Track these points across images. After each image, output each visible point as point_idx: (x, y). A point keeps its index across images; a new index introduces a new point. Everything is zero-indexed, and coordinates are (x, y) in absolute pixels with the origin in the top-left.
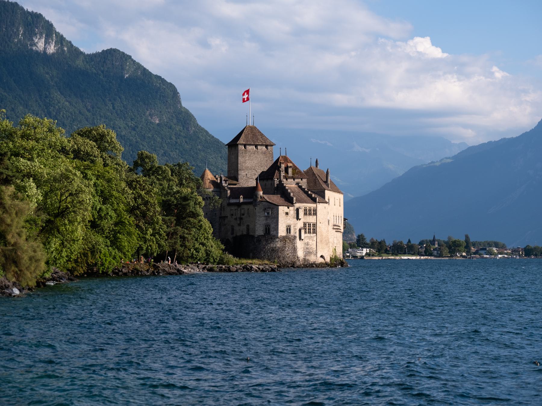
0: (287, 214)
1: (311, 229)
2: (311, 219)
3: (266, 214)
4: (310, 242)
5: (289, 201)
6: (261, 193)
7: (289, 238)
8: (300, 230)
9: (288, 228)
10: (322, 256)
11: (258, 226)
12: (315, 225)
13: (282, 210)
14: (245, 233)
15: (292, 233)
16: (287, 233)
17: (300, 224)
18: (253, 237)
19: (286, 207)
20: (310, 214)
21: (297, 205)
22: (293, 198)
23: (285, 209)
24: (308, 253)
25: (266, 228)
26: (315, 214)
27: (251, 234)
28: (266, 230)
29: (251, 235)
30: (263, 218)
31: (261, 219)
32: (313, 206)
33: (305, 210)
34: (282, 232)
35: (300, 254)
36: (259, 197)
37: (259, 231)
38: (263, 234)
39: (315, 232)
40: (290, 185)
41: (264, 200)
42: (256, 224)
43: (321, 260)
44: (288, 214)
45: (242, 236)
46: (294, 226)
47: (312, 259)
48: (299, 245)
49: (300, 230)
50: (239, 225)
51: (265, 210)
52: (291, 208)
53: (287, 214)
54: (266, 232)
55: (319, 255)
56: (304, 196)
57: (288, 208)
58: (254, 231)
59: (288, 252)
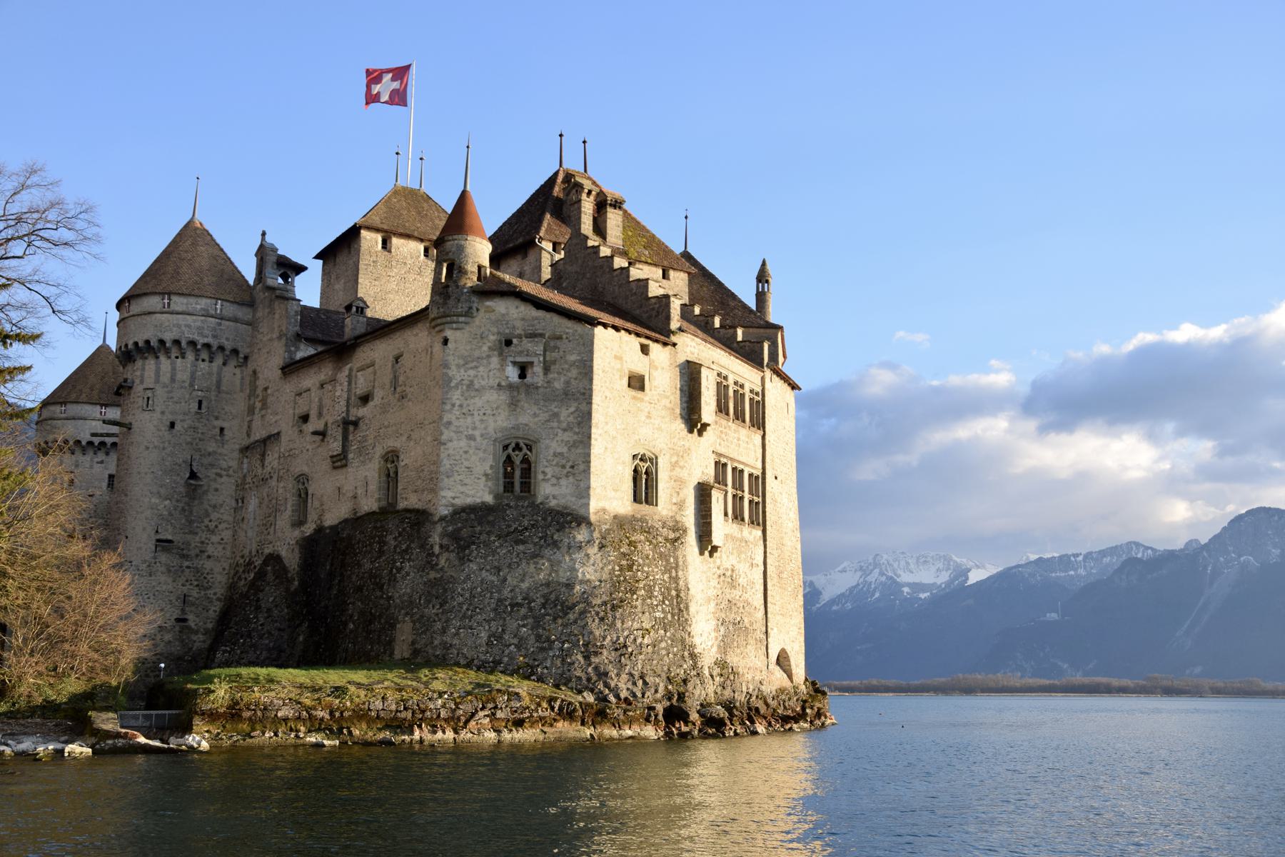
0: (637, 382)
3: (512, 373)
7: (648, 531)
9: (644, 466)
11: (456, 445)
16: (636, 499)
18: (420, 518)
19: (633, 343)
25: (509, 460)
27: (409, 500)
28: (508, 476)
29: (407, 510)
30: (492, 396)
31: (478, 402)
36: (472, 268)
38: (489, 499)
41: (504, 288)
42: (446, 435)
44: (642, 388)
46: (674, 465)
53: (637, 382)
54: (509, 487)
57: (645, 350)
58: (432, 483)
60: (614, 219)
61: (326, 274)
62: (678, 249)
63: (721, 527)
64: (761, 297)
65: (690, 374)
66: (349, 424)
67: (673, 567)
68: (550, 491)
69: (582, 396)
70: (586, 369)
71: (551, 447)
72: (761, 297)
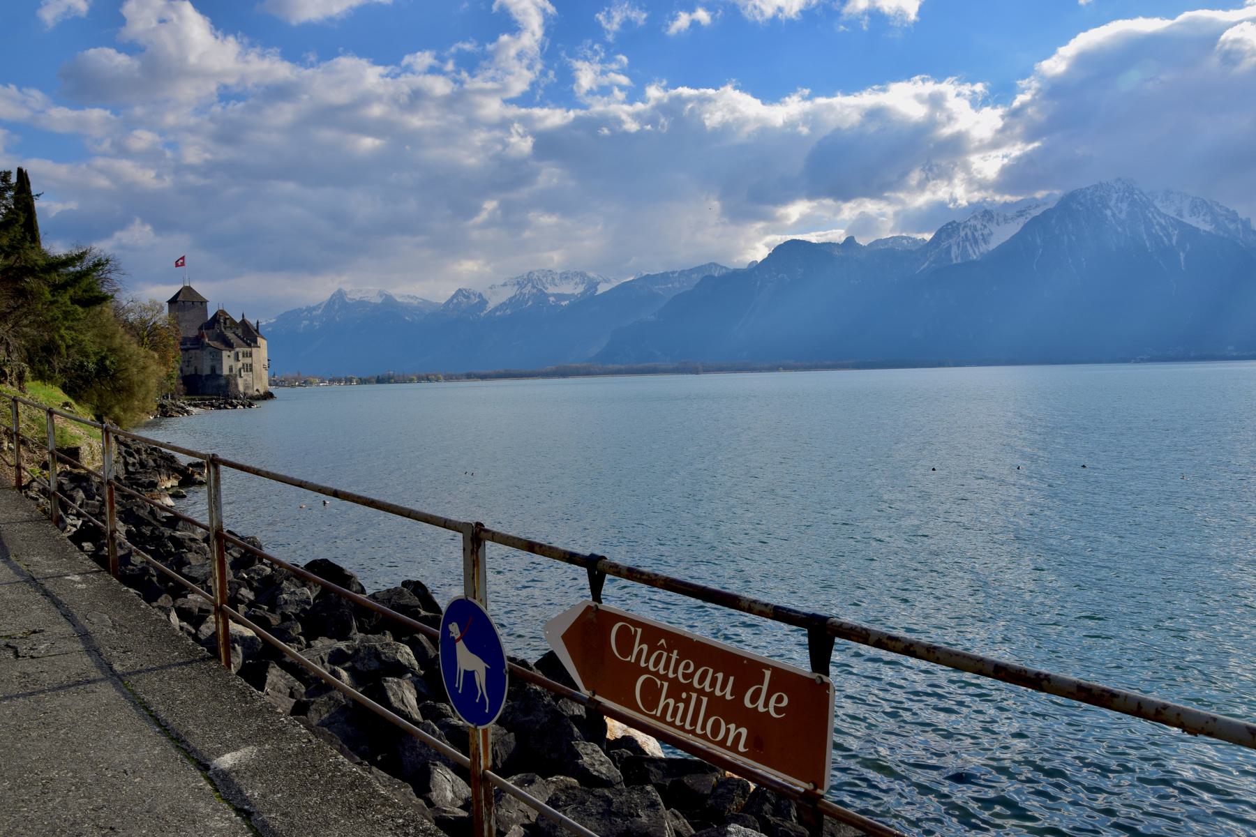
0: (229, 356)
1: (249, 368)
2: (248, 361)
4: (248, 379)
5: (230, 346)
6: (207, 340)
8: (240, 370)
10: (257, 390)
12: (251, 365)
13: (225, 354)
14: (193, 373)
15: (234, 372)
17: (240, 365)
18: (201, 376)
20: (247, 356)
21: (237, 349)
22: (233, 344)
23: (228, 353)
24: (246, 387)
26: (251, 356)
32: (249, 349)
33: (243, 353)
34: (226, 372)
35: (241, 388)
37: (207, 371)
39: (251, 370)
40: (230, 335)
43: (257, 393)
45: (191, 375)
47: (250, 392)
48: (240, 381)
49: (240, 370)
50: (188, 366)
51: (211, 353)
52: (233, 352)
53: (229, 356)
55: (255, 389)
56: (241, 342)
59: (232, 388)
60: (228, 322)
61: (169, 307)
62: (238, 320)
63: (243, 374)
64: (258, 327)
65: (237, 355)
66: (189, 361)
67: (235, 380)
68: (218, 372)
69: (221, 360)
70: (222, 357)
71: (218, 366)
72: (258, 327)
